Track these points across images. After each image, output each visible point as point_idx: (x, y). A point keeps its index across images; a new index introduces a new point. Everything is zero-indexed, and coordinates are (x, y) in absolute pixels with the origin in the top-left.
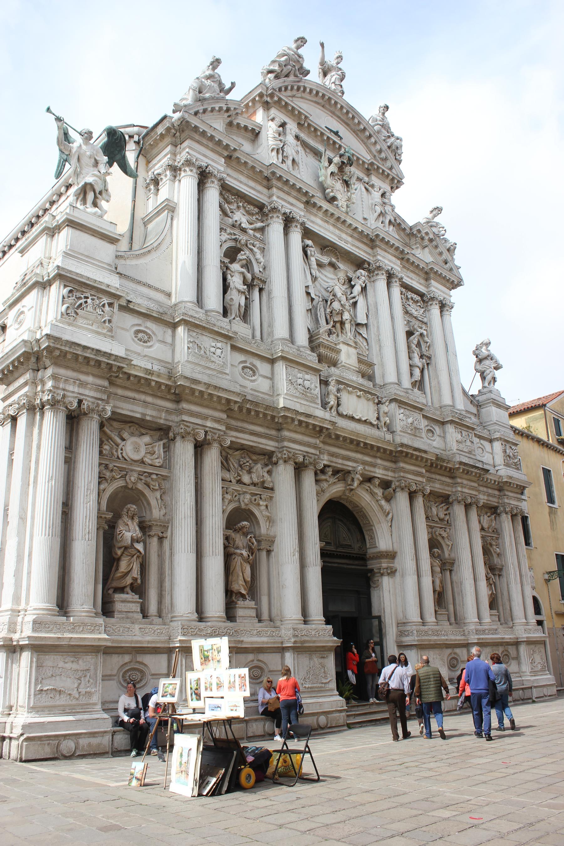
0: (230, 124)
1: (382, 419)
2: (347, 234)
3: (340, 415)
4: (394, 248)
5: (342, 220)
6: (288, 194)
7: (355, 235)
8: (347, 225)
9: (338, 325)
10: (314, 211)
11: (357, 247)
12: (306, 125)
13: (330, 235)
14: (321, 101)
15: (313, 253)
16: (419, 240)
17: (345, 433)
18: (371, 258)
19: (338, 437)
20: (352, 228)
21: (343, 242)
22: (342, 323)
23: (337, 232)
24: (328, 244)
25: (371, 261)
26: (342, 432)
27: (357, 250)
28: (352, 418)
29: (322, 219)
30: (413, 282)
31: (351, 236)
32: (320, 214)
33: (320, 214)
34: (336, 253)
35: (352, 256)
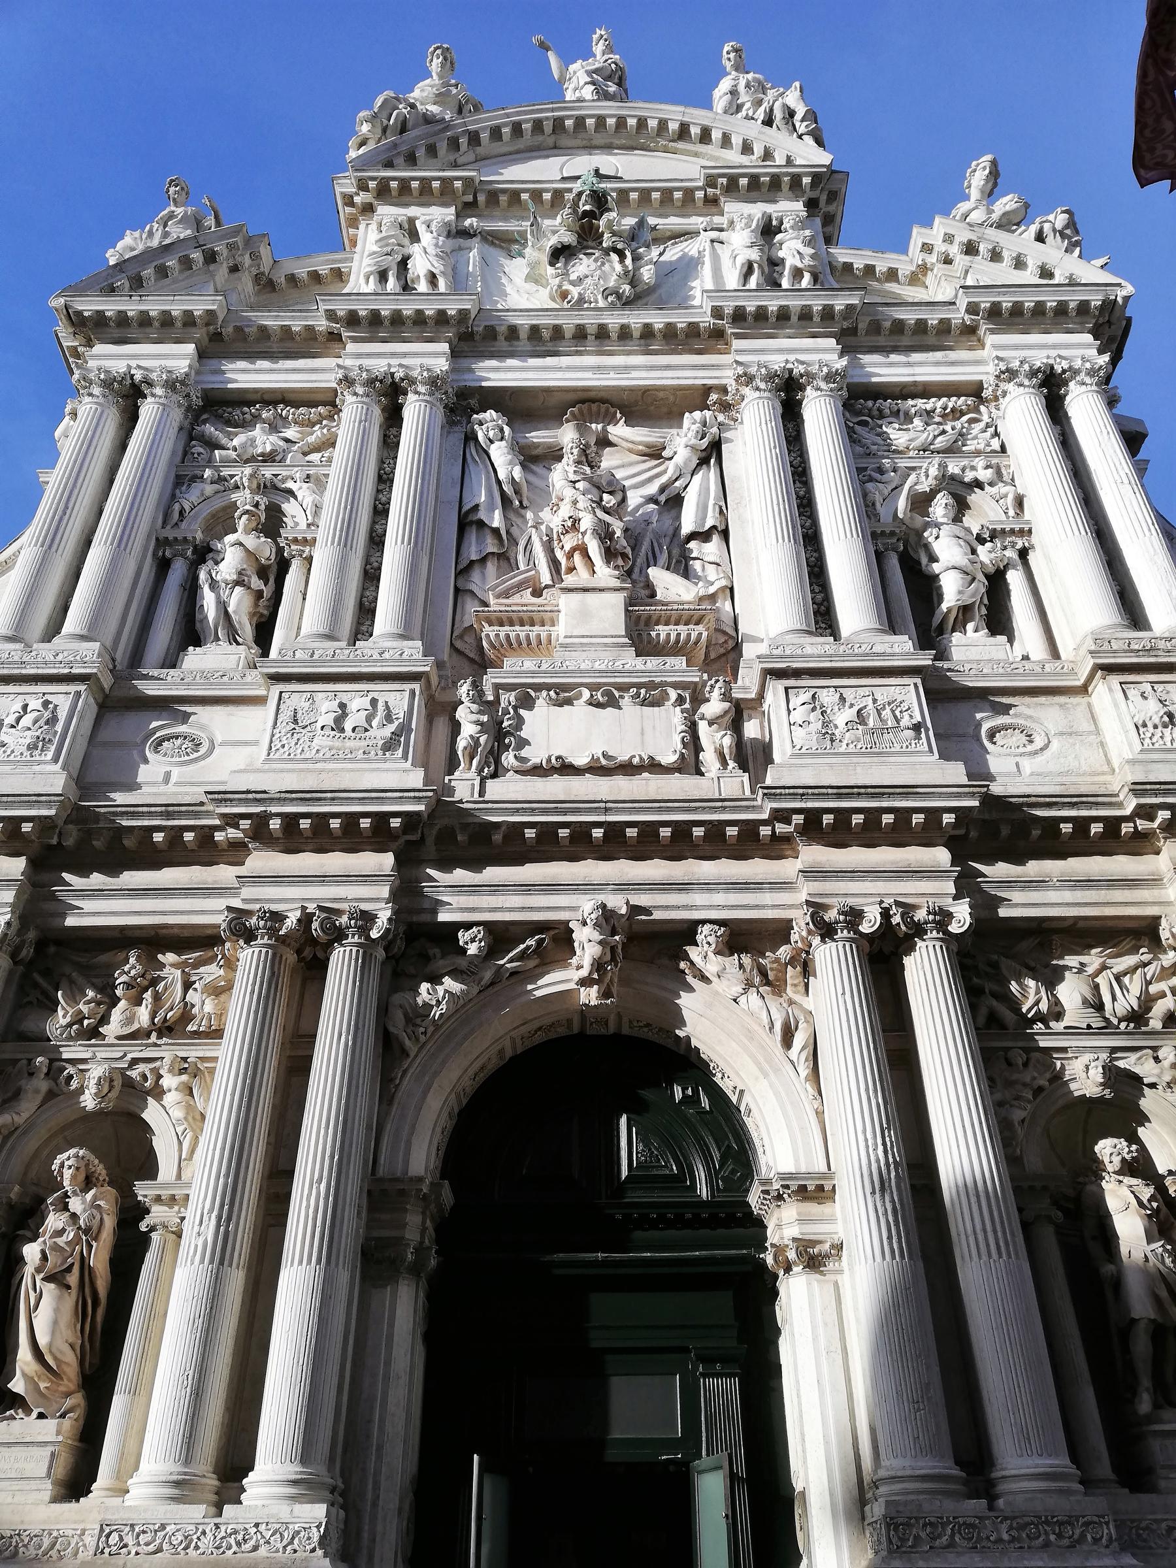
0: (266, 285)
2: (629, 353)
4: (794, 319)
5: (592, 330)
8: (614, 336)
9: (577, 557)
10: (502, 344)
12: (481, 198)
13: (559, 375)
14: (541, 138)
16: (940, 269)
20: (636, 334)
21: (612, 375)
24: (572, 397)
25: (724, 382)
28: (566, 769)
30: (918, 370)
34: (607, 410)
35: (661, 394)
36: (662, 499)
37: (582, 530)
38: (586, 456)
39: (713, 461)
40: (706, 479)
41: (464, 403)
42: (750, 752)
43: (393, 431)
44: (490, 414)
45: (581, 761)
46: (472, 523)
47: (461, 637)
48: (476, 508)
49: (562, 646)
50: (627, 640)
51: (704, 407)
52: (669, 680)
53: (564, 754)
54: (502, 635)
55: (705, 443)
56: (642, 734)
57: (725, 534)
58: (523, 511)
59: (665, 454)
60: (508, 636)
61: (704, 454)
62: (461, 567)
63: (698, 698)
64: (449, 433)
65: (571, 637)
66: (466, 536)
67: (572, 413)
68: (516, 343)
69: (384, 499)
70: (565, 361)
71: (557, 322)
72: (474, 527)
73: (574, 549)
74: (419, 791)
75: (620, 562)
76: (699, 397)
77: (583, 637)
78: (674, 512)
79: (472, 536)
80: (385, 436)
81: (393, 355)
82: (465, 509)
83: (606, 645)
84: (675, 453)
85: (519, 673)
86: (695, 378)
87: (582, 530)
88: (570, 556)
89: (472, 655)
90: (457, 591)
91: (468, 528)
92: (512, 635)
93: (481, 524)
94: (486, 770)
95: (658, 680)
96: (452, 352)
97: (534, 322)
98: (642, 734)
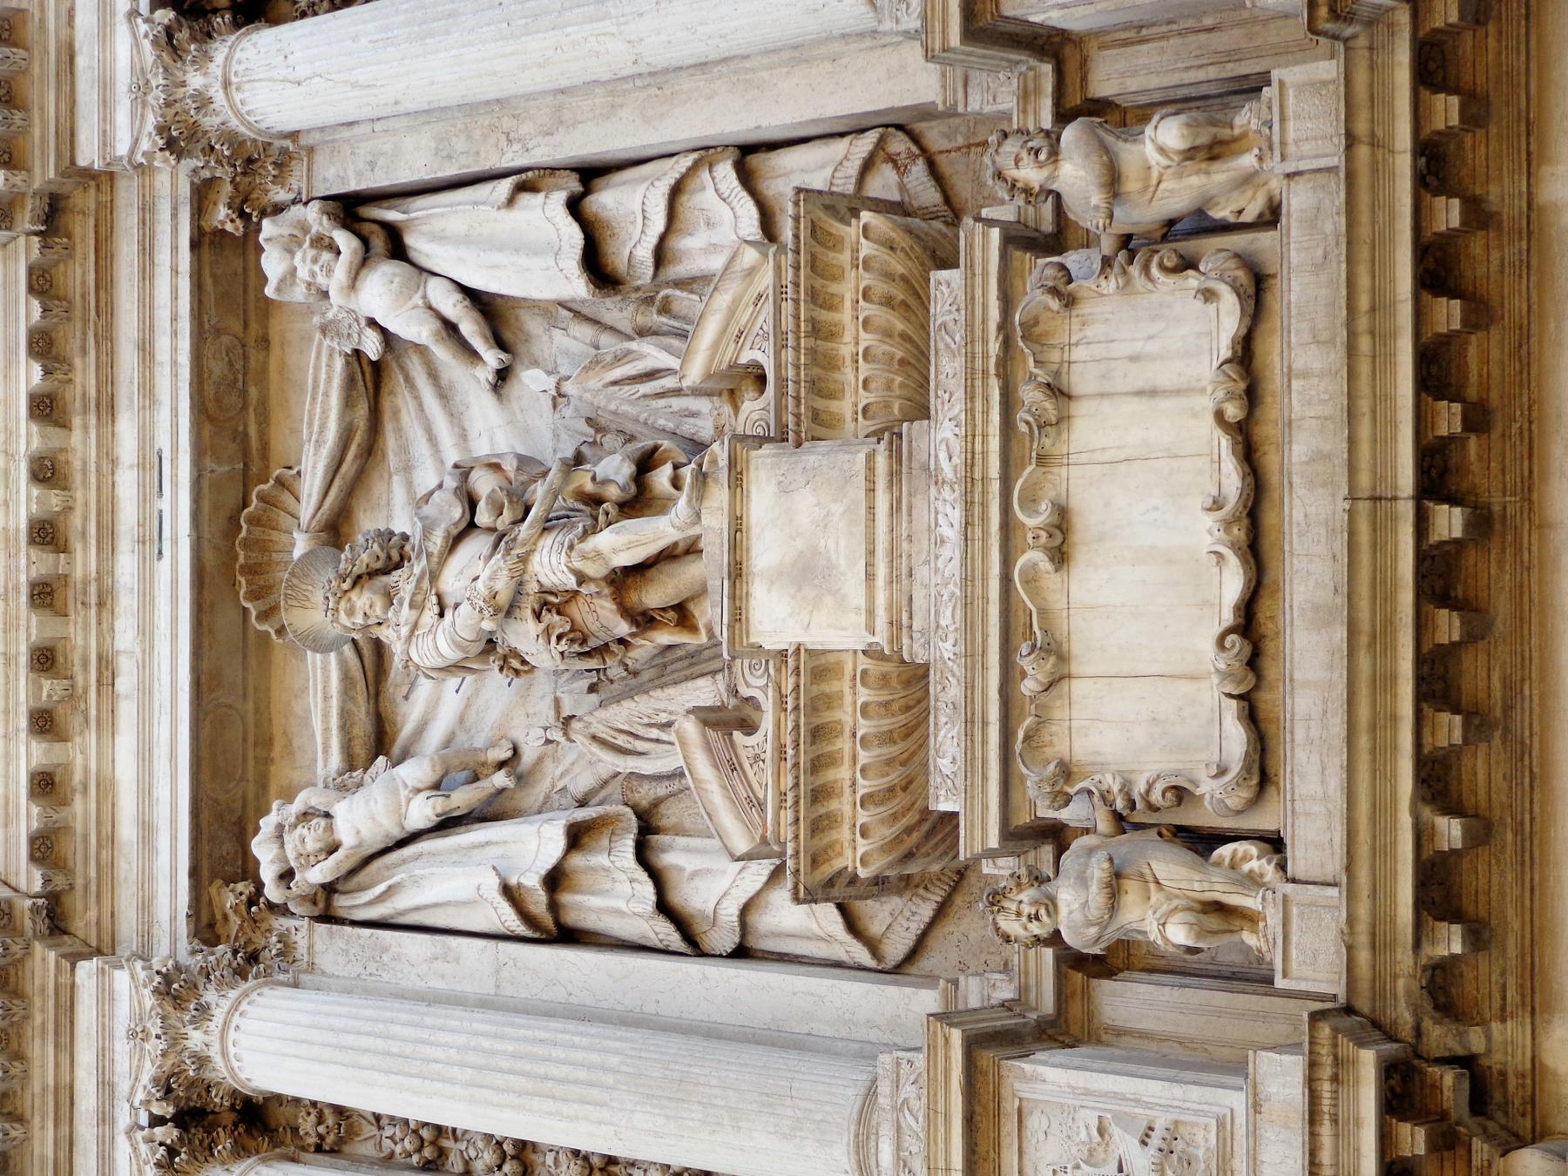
1: (1177, 194)
2: (109, 458)
3: (1262, 771)
5: (42, 563)
6: (65, 1096)
7: (84, 377)
8: (55, 499)
9: (655, 595)
11: (146, 350)
15: (310, 837)
17: (1382, 810)
18: (163, 181)
19: (1439, 888)
21: (165, 504)
22: (624, 579)
23: (126, 566)
25: (185, 190)
26: (1383, 852)
27: (163, 344)
29: (107, 724)
31: (107, 407)
32: (81, 754)
33: (81, 754)
34: (254, 521)
35: (217, 368)
36: (492, 358)
37: (571, 582)
38: (372, 574)
39: (392, 215)
40: (439, 238)
41: (235, 921)
42: (1212, 73)
43: (307, 1124)
44: (262, 849)
45: (1233, 584)
46: (554, 906)
47: (873, 946)
48: (510, 893)
49: (895, 639)
50: (883, 445)
51: (248, 245)
52: (994, 314)
53: (1217, 630)
54: (863, 817)
55: (343, 239)
56: (1152, 393)
57: (591, 174)
58: (528, 757)
59: (372, 346)
60: (866, 801)
61: (379, 242)
62: (674, 939)
63: (1046, 236)
64: (312, 966)
65: (871, 613)
66: (589, 921)
67: (264, 616)
68: (78, 776)
69: (489, 1157)
70: (125, 636)
71: (23, 660)
72: (566, 898)
73: (626, 612)
74: (1313, 1065)
75: (661, 478)
76: (224, 260)
77: (870, 577)
78: (533, 324)
79: (585, 908)
80: (319, 1149)
81: (105, 1118)
82: (515, 924)
83: (895, 509)
84: (372, 323)
85: (972, 761)
86: (175, 271)
87: (571, 582)
88: (645, 621)
89: (926, 911)
90: (742, 952)
91: (572, 918)
92: (864, 786)
93: (555, 880)
94: (1254, 865)
95: (994, 347)
96: (99, 952)
97: (23, 723)
98: (1152, 393)
